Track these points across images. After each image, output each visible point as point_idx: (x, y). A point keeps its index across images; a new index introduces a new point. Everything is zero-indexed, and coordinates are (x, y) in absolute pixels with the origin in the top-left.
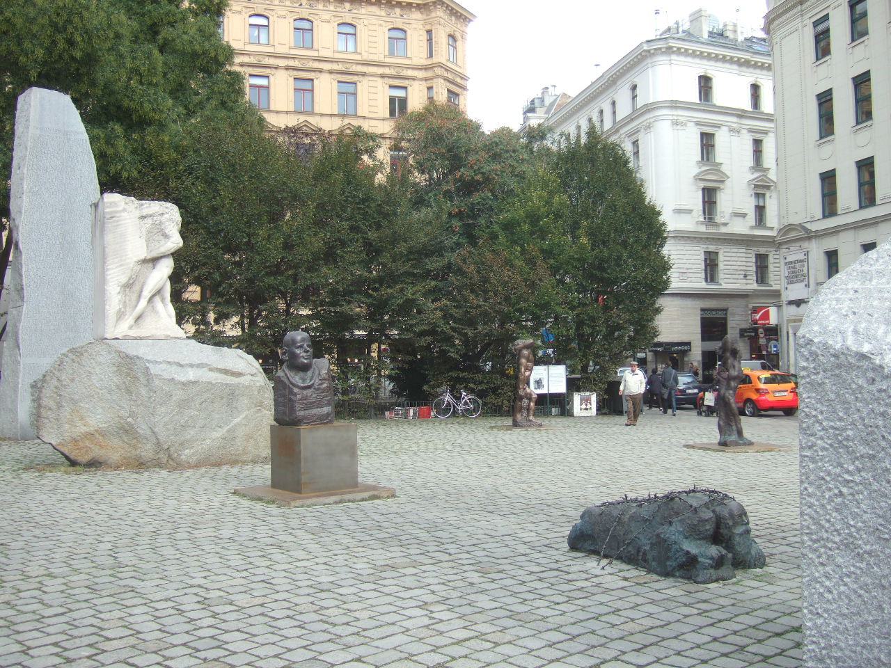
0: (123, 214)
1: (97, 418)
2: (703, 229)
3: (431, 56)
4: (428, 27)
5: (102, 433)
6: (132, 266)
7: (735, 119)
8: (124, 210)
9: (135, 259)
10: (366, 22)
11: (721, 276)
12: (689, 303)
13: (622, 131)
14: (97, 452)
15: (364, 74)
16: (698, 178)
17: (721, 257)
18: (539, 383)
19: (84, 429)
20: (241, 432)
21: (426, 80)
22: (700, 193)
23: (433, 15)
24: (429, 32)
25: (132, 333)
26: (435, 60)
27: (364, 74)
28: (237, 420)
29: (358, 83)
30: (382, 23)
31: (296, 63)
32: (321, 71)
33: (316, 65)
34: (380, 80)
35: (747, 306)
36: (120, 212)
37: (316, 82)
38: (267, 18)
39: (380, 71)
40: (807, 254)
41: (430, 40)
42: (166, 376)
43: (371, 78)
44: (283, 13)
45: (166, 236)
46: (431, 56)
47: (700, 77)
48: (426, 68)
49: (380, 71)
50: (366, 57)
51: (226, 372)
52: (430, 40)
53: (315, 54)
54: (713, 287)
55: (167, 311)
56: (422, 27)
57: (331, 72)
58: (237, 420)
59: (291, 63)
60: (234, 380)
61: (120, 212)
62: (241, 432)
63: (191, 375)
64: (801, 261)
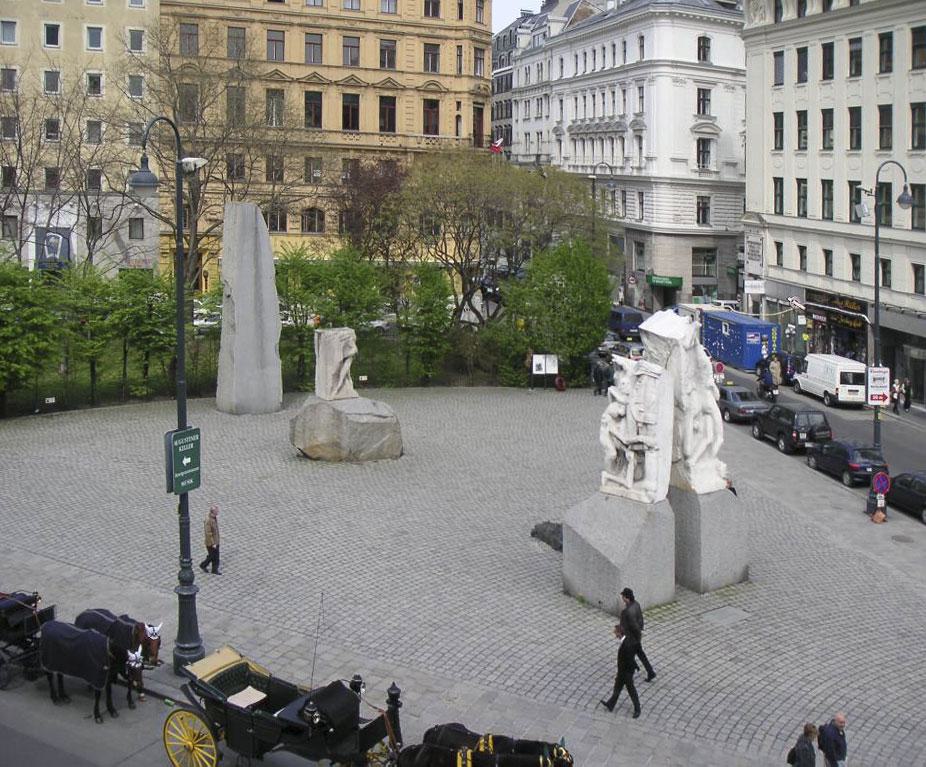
1: (322, 438)
2: (695, 176)
3: (461, 17)
5: (323, 444)
7: (729, 77)
11: (712, 217)
12: (682, 242)
13: (630, 74)
14: (320, 453)
15: (403, 34)
16: (694, 130)
17: (712, 202)
18: (539, 367)
19: (317, 443)
20: (386, 444)
22: (695, 144)
25: (338, 396)
26: (466, 22)
27: (403, 34)
28: (384, 439)
31: (346, 24)
32: (367, 31)
33: (362, 26)
34: (416, 38)
35: (735, 246)
40: (762, 239)
42: (355, 420)
45: (351, 347)
46: (461, 17)
47: (699, 39)
50: (406, 18)
51: (380, 416)
53: (361, 15)
54: (705, 229)
55: (350, 383)
57: (375, 32)
58: (384, 439)
60: (383, 420)
62: (386, 444)
63: (365, 419)
64: (757, 243)
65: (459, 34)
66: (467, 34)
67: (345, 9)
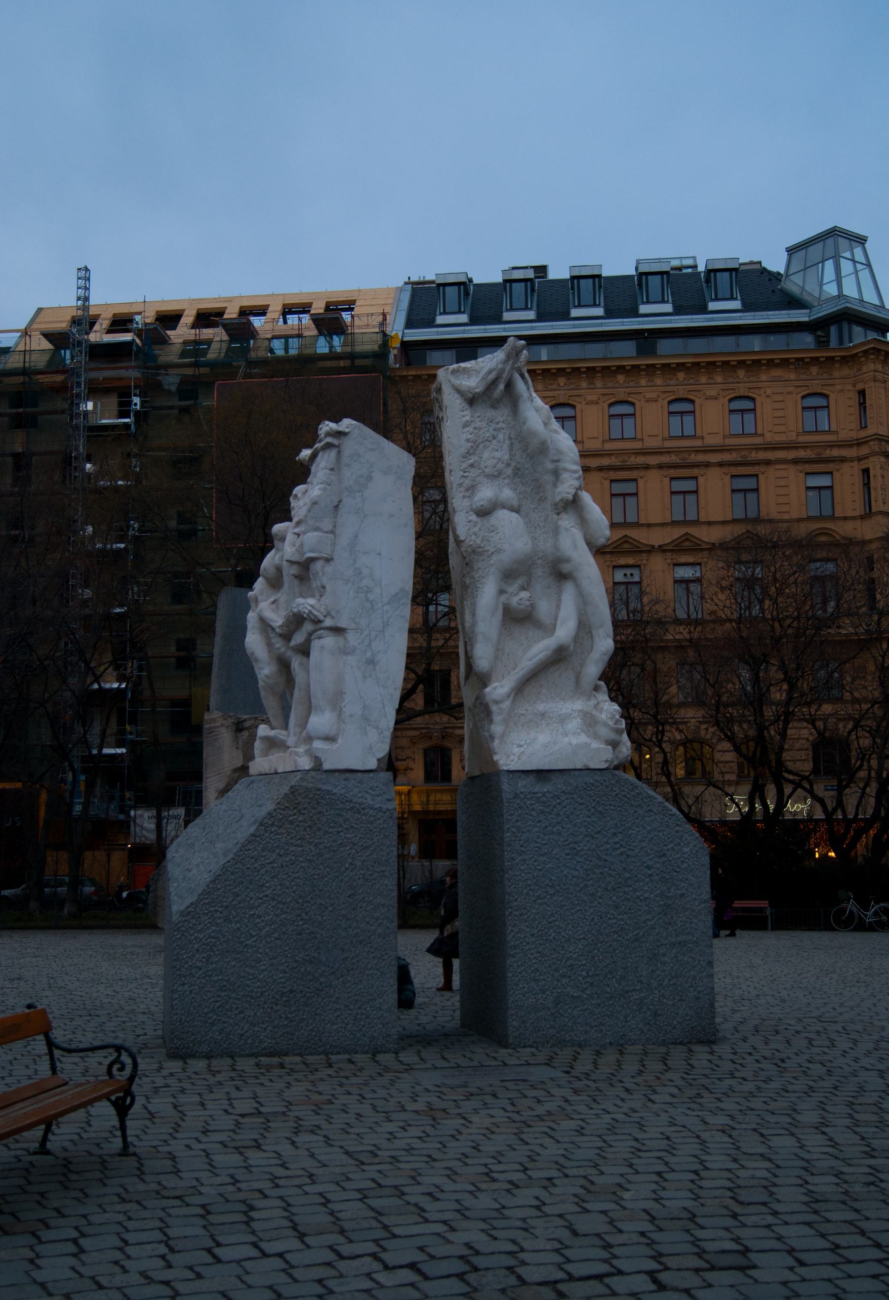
0: (221, 729)
4: (860, 386)
6: (229, 773)
8: (222, 725)
9: (232, 768)
10: (769, 391)
15: (768, 463)
21: (860, 459)
23: (865, 369)
24: (862, 393)
26: (871, 430)
27: (768, 463)
29: (760, 476)
30: (791, 389)
31: (673, 459)
33: (701, 458)
36: (218, 727)
37: (701, 480)
38: (633, 404)
39: (791, 455)
41: (862, 405)
43: (777, 467)
44: (654, 395)
46: (863, 427)
48: (859, 443)
49: (791, 455)
50: (769, 437)
52: (862, 405)
56: (850, 387)
57: (721, 464)
59: (665, 459)
61: (218, 727)
65: (864, 450)
66: (875, 446)
67: (671, 438)
